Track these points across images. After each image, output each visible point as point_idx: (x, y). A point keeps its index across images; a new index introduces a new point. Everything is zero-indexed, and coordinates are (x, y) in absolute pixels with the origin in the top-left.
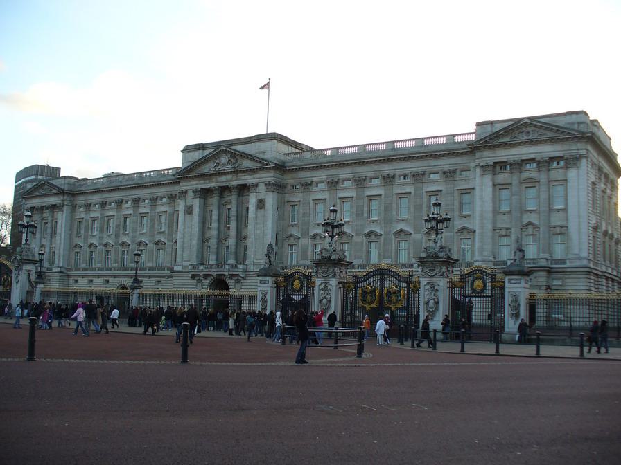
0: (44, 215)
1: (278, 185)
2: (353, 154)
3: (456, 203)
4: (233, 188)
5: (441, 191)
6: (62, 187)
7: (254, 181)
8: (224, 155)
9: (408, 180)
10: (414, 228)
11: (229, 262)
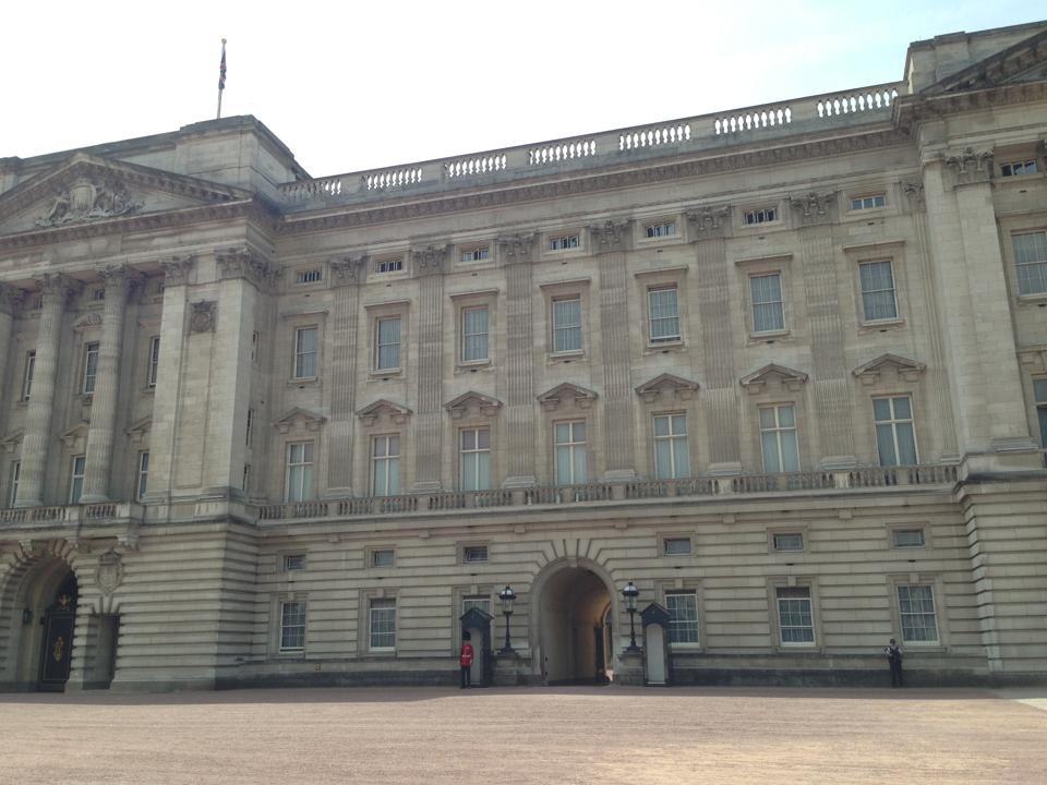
5: (790, 258)
7: (183, 251)
9: (678, 235)
10: (707, 371)
11: (83, 498)
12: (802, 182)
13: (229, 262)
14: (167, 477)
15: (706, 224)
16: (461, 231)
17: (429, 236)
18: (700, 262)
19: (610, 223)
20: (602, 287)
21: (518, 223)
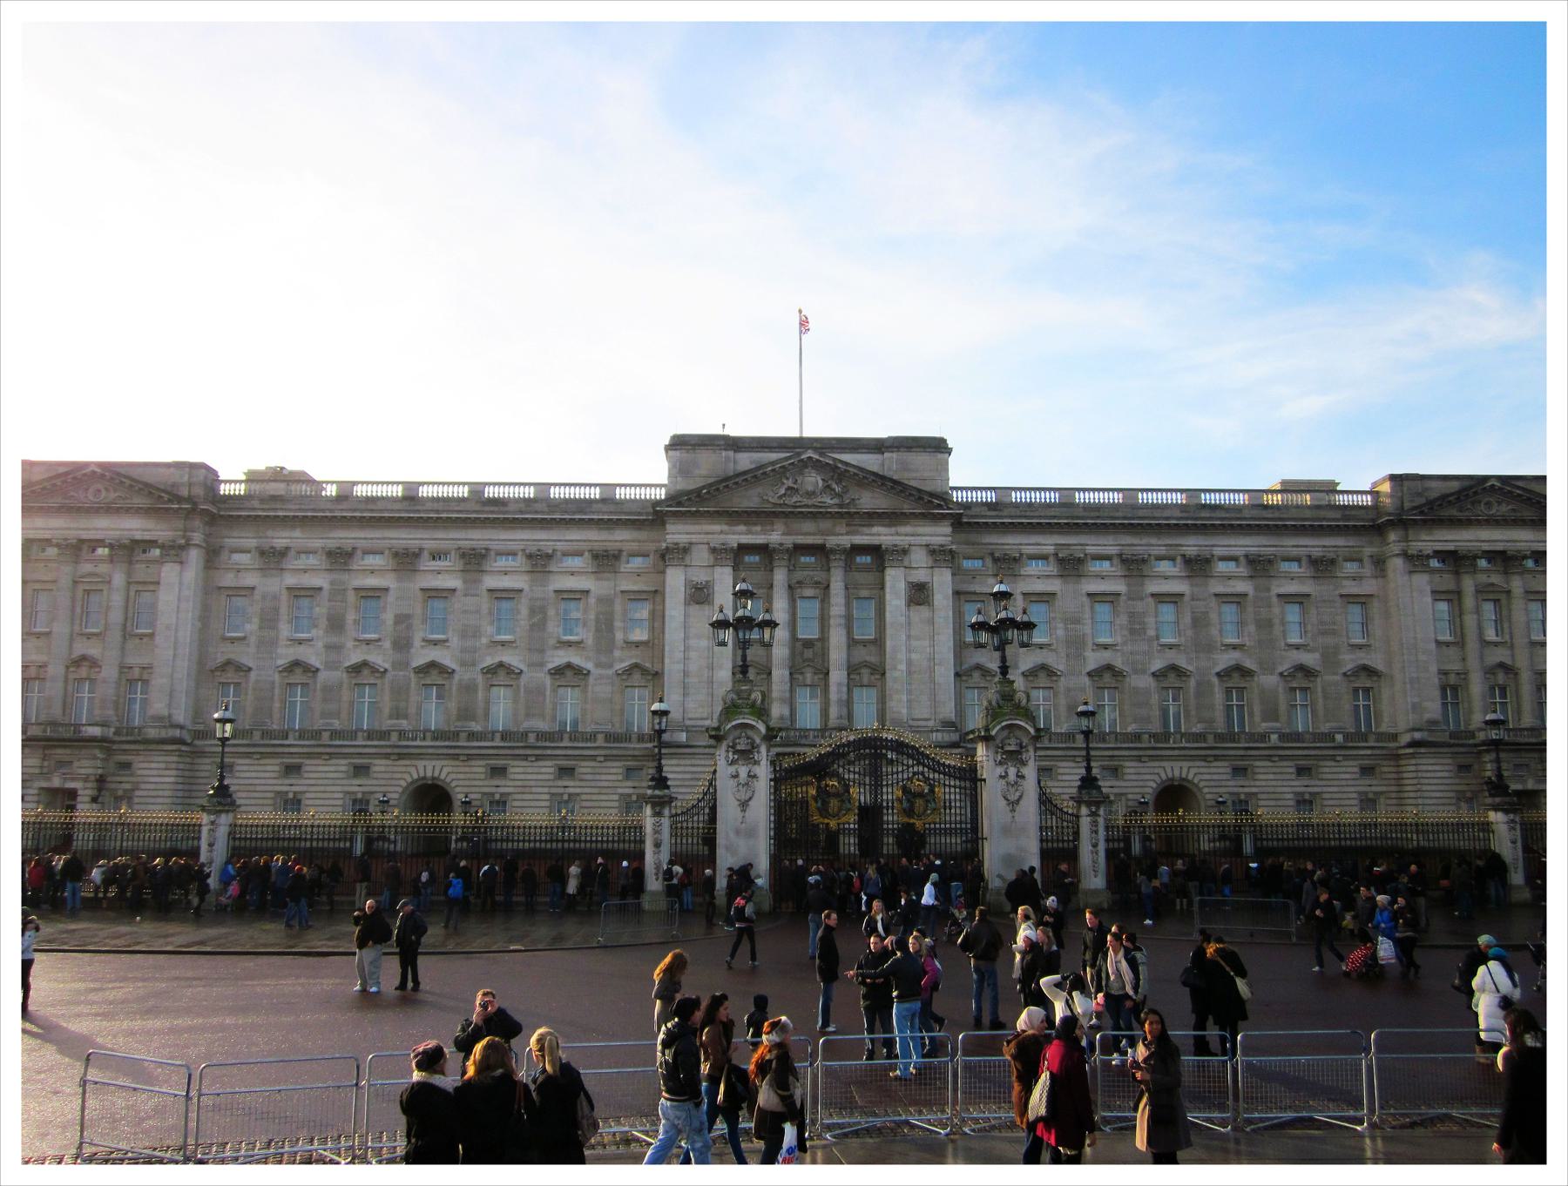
0: (87, 568)
2: (1115, 507)
6: (185, 492)
11: (833, 722)
14: (904, 711)
15: (1259, 566)
18: (1256, 589)
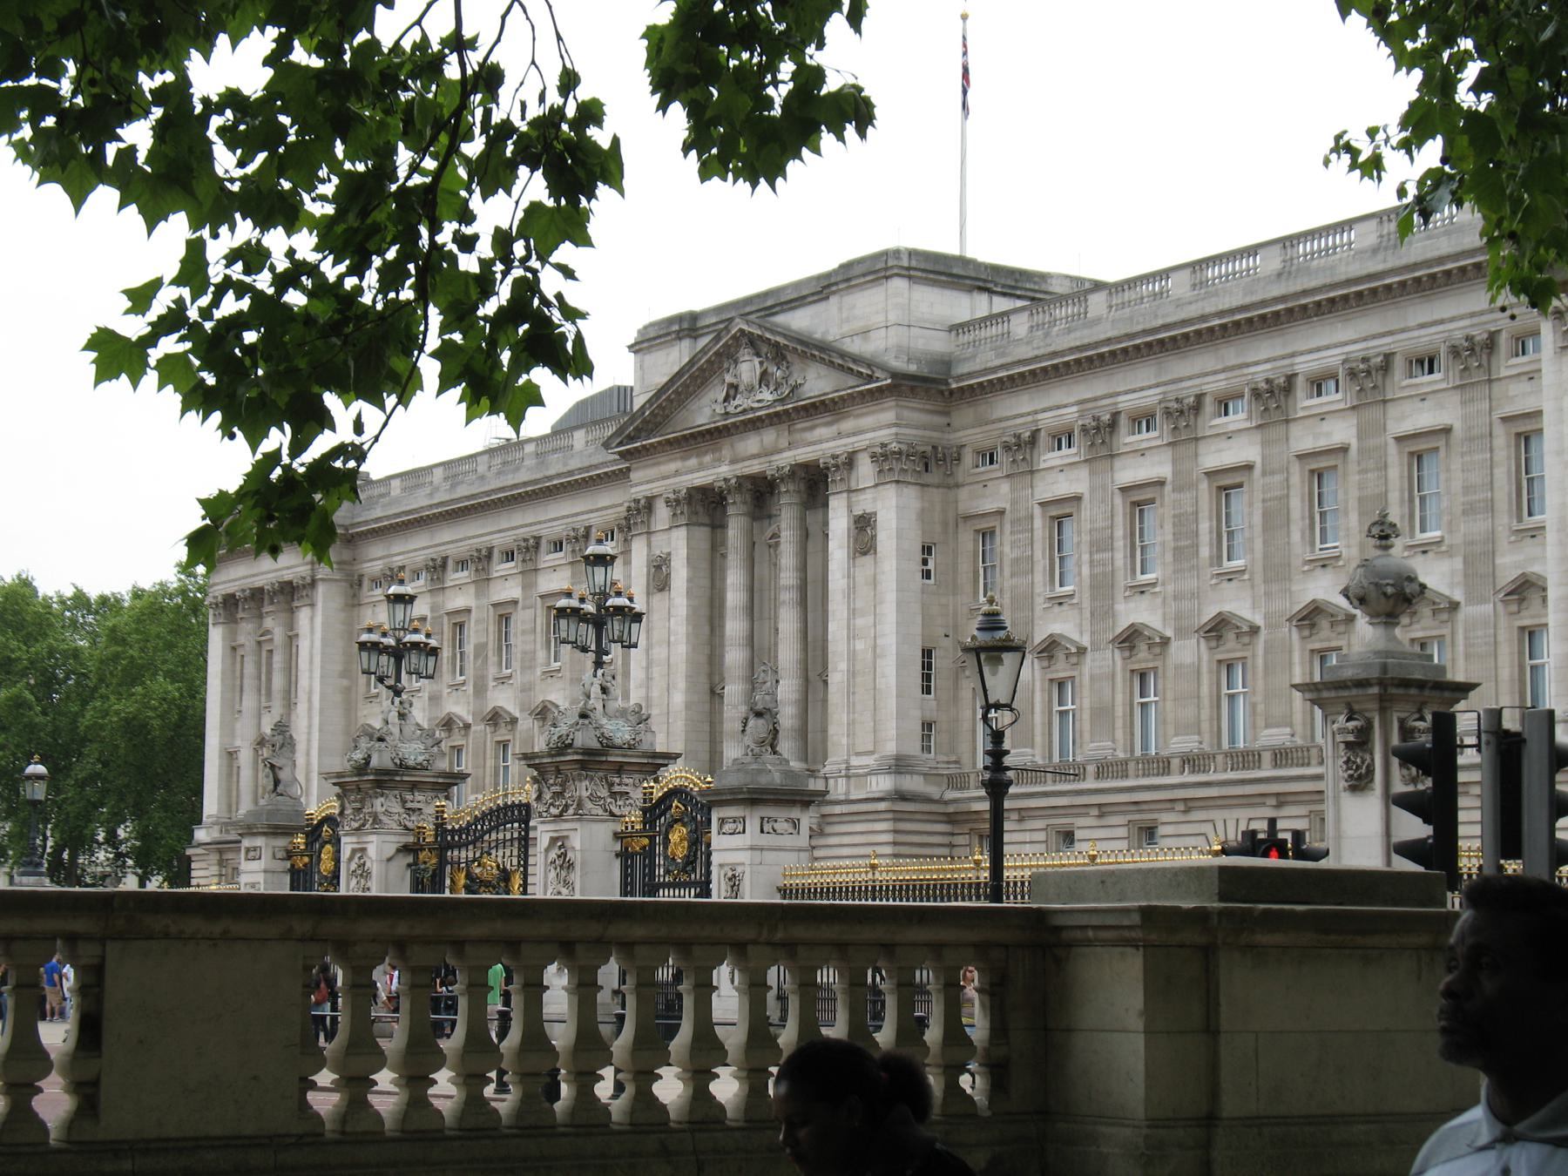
1: (923, 455)
3: (1503, 476)
4: (782, 480)
5: (1447, 431)
7: (840, 446)
8: (745, 354)
12: (1461, 318)
13: (883, 457)
14: (844, 741)
16: (1126, 393)
17: (1095, 399)
19: (1268, 381)
20: (1264, 474)
21: (1181, 380)
